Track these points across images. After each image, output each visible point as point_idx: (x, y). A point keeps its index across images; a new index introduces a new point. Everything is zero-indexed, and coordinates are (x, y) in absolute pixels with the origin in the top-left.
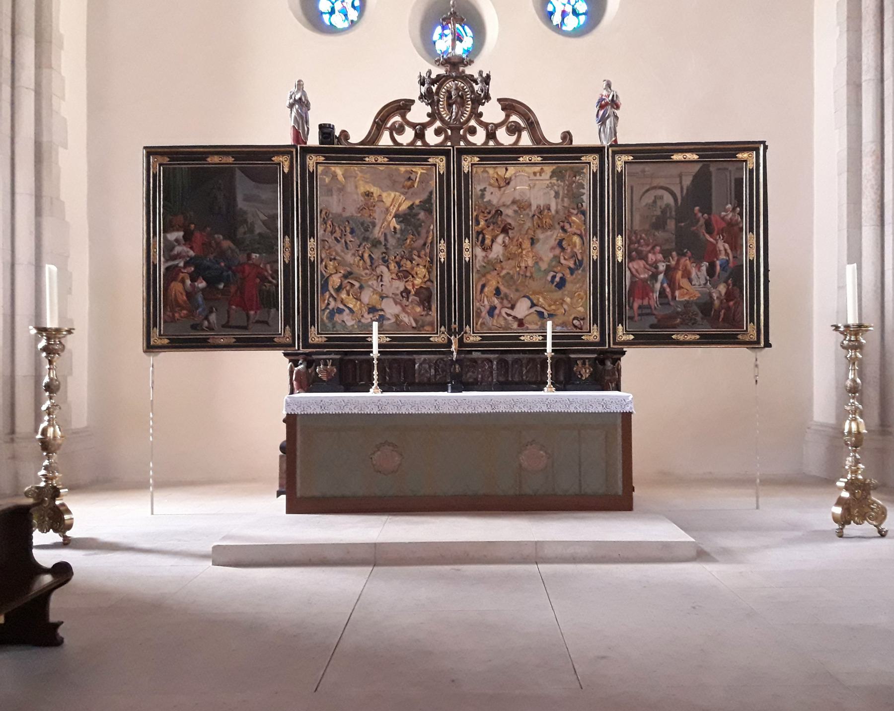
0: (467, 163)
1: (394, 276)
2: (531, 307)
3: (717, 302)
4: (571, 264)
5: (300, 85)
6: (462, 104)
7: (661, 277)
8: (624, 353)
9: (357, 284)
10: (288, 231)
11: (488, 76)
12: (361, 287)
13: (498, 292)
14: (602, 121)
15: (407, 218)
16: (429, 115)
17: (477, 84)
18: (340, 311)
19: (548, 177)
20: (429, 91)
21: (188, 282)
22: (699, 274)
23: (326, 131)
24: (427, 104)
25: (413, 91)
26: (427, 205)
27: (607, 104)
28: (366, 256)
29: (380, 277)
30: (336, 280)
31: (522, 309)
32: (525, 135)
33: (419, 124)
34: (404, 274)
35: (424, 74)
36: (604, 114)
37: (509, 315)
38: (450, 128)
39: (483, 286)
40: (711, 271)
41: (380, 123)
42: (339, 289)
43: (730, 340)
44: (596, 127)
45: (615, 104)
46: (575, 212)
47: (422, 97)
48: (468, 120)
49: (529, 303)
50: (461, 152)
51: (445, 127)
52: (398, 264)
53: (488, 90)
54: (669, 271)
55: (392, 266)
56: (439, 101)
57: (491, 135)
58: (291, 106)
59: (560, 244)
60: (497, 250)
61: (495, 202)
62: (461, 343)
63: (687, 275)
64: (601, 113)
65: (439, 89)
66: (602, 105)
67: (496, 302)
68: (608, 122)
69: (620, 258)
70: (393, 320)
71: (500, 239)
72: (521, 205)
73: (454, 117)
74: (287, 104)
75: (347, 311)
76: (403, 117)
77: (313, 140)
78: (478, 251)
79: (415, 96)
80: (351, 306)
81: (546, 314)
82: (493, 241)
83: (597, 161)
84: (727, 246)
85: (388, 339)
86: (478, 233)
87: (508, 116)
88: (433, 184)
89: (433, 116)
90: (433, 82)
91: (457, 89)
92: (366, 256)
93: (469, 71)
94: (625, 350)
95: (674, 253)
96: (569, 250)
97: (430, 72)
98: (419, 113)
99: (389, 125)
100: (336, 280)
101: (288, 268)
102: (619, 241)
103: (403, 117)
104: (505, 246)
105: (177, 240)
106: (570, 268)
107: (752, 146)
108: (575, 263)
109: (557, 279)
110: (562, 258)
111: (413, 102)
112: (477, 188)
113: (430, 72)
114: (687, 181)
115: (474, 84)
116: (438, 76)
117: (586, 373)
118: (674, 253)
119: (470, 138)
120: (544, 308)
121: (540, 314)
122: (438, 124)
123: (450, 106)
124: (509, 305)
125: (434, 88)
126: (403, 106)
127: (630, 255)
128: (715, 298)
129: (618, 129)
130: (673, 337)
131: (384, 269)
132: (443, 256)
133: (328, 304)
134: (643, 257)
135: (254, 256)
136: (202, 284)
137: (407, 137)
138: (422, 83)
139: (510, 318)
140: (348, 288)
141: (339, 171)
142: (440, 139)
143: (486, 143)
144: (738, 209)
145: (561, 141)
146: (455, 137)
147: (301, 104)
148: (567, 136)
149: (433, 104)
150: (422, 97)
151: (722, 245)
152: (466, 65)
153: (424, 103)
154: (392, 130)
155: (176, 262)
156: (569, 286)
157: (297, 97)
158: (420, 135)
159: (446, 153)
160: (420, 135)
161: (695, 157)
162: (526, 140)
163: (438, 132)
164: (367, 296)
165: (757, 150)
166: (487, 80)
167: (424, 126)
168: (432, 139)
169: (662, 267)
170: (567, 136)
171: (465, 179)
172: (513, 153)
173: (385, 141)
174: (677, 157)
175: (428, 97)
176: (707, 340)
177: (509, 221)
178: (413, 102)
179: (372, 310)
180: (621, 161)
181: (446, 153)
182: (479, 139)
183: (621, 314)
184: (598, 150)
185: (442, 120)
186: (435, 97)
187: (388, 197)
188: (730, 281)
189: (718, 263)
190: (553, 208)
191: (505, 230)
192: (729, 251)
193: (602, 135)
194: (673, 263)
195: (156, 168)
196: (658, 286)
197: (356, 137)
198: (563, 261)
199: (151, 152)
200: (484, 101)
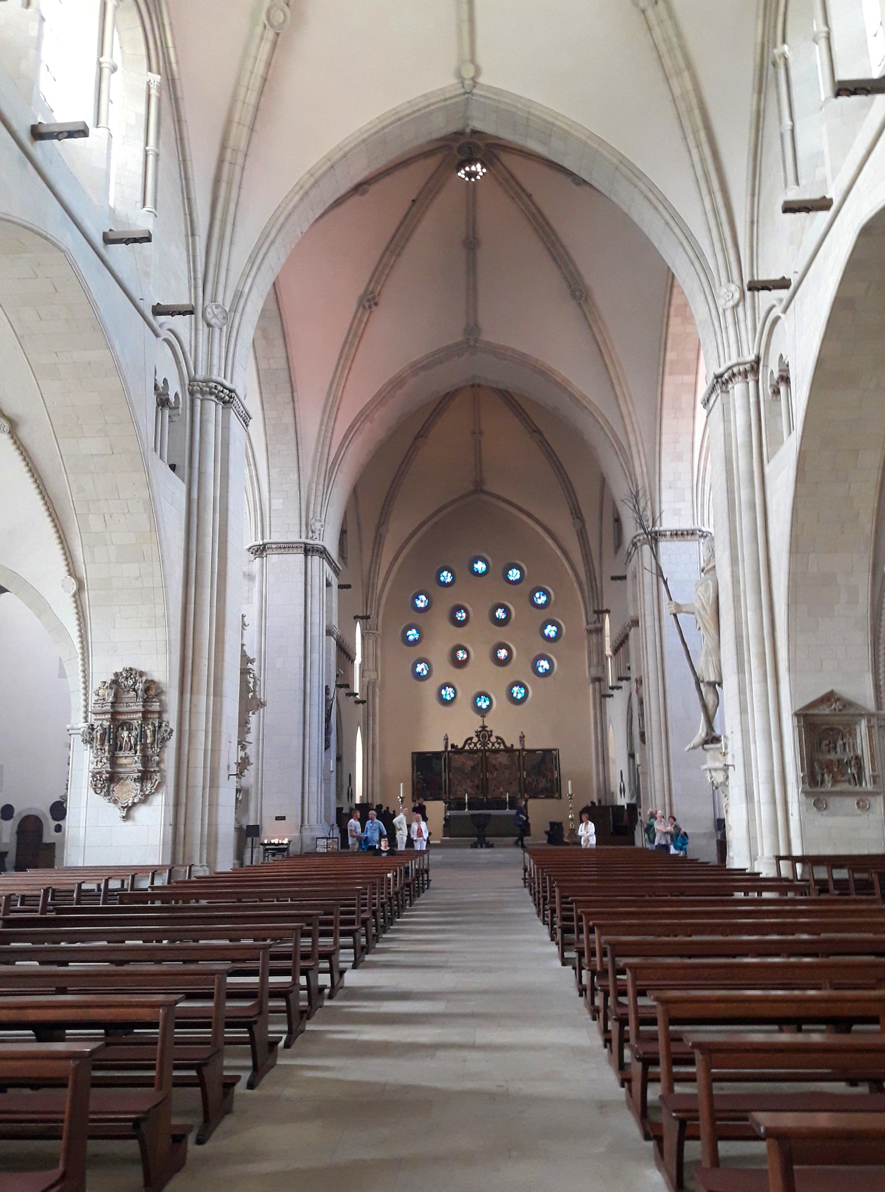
0: (487, 754)
5: (446, 735)
6: (486, 737)
10: (445, 771)
13: (495, 785)
14: (521, 741)
15: (473, 767)
22: (544, 780)
23: (453, 746)
25: (473, 735)
26: (478, 764)
30: (456, 783)
31: (502, 789)
34: (472, 781)
42: (457, 785)
43: (552, 797)
50: (486, 751)
57: (493, 745)
60: (495, 775)
62: (487, 798)
66: (520, 737)
72: (501, 764)
77: (449, 749)
88: (479, 759)
89: (479, 740)
93: (488, 729)
98: (475, 740)
100: (456, 783)
107: (555, 750)
112: (490, 760)
126: (471, 739)
127: (528, 775)
141: (456, 756)
146: (484, 746)
147: (446, 739)
148: (512, 745)
149: (479, 738)
151: (549, 774)
158: (475, 745)
160: (475, 745)
162: (502, 747)
164: (464, 787)
166: (491, 732)
168: (479, 746)
170: (512, 745)
171: (487, 758)
172: (497, 751)
173: (467, 748)
175: (478, 736)
176: (547, 797)
179: (465, 790)
180: (524, 753)
184: (518, 750)
187: (468, 762)
195: (414, 757)
197: (460, 746)
199: (413, 753)
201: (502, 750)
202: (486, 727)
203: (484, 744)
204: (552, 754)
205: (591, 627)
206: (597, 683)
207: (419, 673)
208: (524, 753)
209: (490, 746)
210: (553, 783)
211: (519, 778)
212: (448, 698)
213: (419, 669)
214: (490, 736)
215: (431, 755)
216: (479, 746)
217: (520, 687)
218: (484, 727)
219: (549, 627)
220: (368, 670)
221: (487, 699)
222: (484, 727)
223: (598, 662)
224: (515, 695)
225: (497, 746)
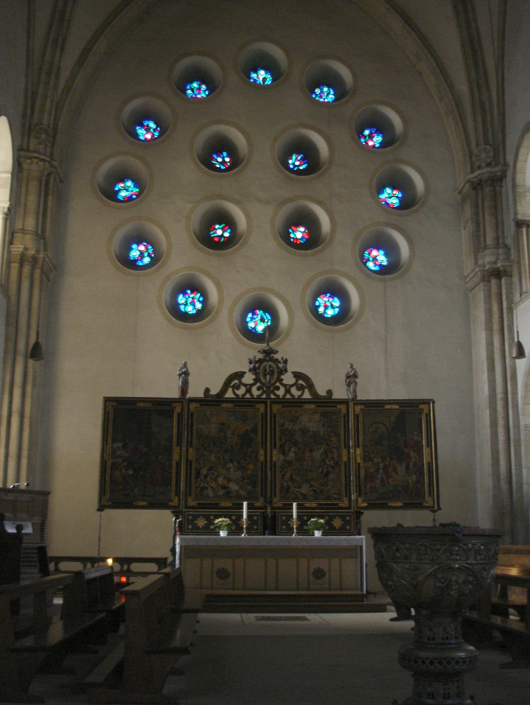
1: (236, 469)
2: (310, 487)
3: (411, 485)
4: (332, 463)
7: (381, 471)
8: (362, 513)
9: (216, 474)
10: (179, 443)
12: (218, 476)
13: (291, 478)
14: (349, 385)
16: (254, 380)
17: (280, 364)
18: (206, 488)
19: (318, 416)
21: (123, 470)
22: (401, 469)
24: (253, 374)
25: (245, 367)
26: (254, 430)
27: (351, 376)
28: (221, 458)
29: (228, 470)
30: (204, 472)
32: (306, 391)
33: (249, 385)
35: (252, 358)
36: (349, 382)
37: (298, 492)
38: (266, 387)
39: (284, 476)
40: (407, 468)
42: (206, 476)
44: (346, 387)
45: (355, 376)
46: (333, 435)
47: (250, 370)
48: (275, 382)
49: (309, 486)
50: (273, 402)
51: (262, 386)
52: (239, 462)
53: (286, 367)
54: (385, 468)
55: (236, 463)
56: (260, 372)
57: (288, 391)
58: (180, 375)
59: (326, 452)
60: (291, 455)
61: (290, 428)
63: (395, 470)
64: (348, 380)
65: (260, 366)
66: (348, 377)
67: (290, 484)
68: (352, 385)
69: (359, 461)
70: (236, 493)
71: (293, 449)
72: (304, 431)
73: (267, 381)
74: (178, 373)
75: (210, 488)
78: (282, 457)
79: (246, 369)
80: (212, 485)
81: (318, 491)
82: (289, 450)
83: (345, 408)
84: (415, 454)
85: (231, 504)
86: (282, 446)
89: (256, 380)
90: (256, 362)
91: (270, 366)
92: (221, 458)
93: (276, 356)
94: (362, 511)
95: (388, 458)
96: (330, 456)
97: (255, 357)
98: (249, 378)
99: (232, 385)
101: (178, 464)
102: (358, 451)
104: (295, 453)
105: (118, 448)
106: (331, 466)
107: (427, 402)
108: (334, 464)
109: (325, 472)
110: (327, 460)
111: (245, 373)
113: (255, 357)
114: (393, 419)
115: (279, 364)
116: (259, 359)
118: (388, 458)
119: (277, 392)
120: (317, 488)
121: (315, 491)
122: (259, 384)
123: (265, 376)
124: (297, 486)
125: (257, 365)
126: (239, 375)
128: (410, 483)
129: (357, 389)
130: (389, 504)
131: (230, 465)
132: (262, 458)
133: (200, 484)
134: (371, 460)
135: (160, 457)
136: (131, 472)
137: (241, 391)
138: (251, 362)
139: (298, 494)
140: (211, 475)
143: (285, 395)
144: (420, 435)
145: (326, 394)
147: (185, 374)
148: (330, 392)
149: (256, 374)
150: (250, 370)
151: (412, 454)
152: (275, 353)
153: (251, 374)
155: (118, 460)
156: (331, 476)
157: (184, 370)
158: (249, 391)
159: (265, 403)
160: (249, 391)
161: (397, 407)
162: (307, 395)
163: (259, 389)
164: (220, 480)
165: (429, 404)
166: (286, 361)
167: (252, 385)
168: (255, 392)
169: (381, 466)
170: (330, 392)
171: (274, 417)
172: (299, 402)
173: (229, 394)
174: (387, 407)
175: (253, 370)
177: (299, 439)
178: (245, 373)
180: (358, 408)
181: (265, 403)
182: (281, 392)
183: (360, 491)
184: (345, 402)
185: (261, 383)
186: (258, 371)
188: (418, 474)
189: (411, 463)
190: (322, 432)
191: (295, 444)
192: (416, 457)
193: (349, 393)
194: (388, 463)
196: (379, 476)
198: (327, 462)
199: (107, 400)
200: (284, 372)
201: (307, 402)
204: (421, 412)
205: (484, 172)
206: (494, 282)
207: (135, 261)
208: (358, 408)
209: (281, 392)
210: (422, 474)
211: (347, 464)
212: (190, 310)
213: (134, 254)
215: (149, 405)
216: (255, 392)
217: (333, 296)
219: (388, 190)
220: (23, 231)
221: (268, 317)
223: (497, 238)
224: (321, 310)
225: (294, 390)
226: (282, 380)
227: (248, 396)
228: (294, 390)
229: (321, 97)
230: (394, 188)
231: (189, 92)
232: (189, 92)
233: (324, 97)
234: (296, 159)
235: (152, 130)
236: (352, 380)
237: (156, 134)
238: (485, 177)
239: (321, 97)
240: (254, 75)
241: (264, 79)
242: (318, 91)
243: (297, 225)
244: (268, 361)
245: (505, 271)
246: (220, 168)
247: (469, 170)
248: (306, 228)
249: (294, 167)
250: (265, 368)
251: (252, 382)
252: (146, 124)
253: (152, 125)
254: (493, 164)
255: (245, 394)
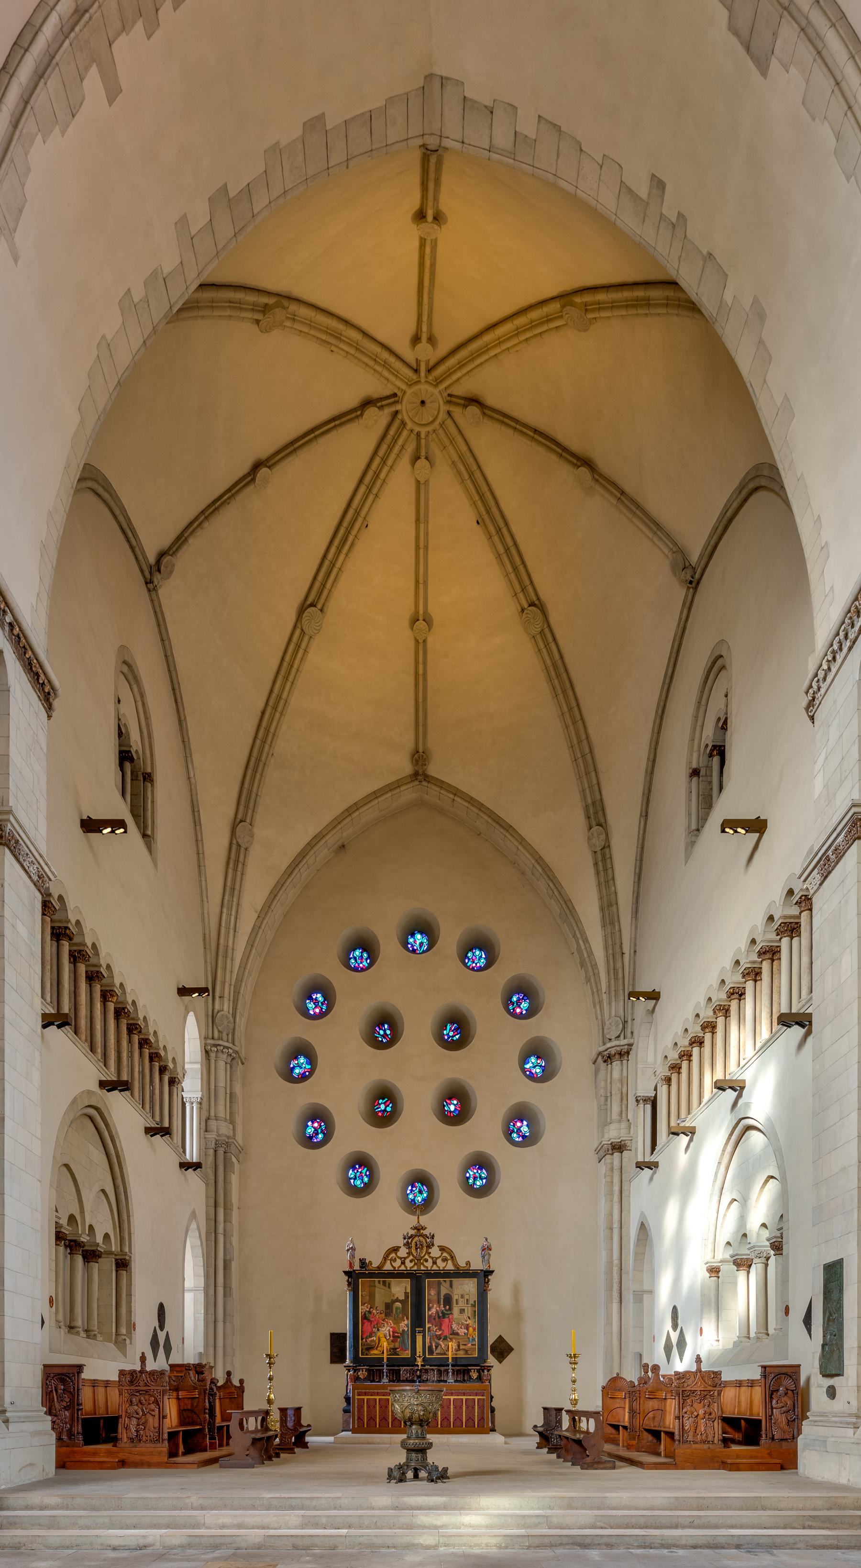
6: (422, 1249)
11: (433, 1235)
14: (483, 1257)
20: (408, 1242)
23: (363, 1263)
25: (400, 1242)
32: (450, 1262)
41: (385, 1258)
44: (481, 1259)
47: (404, 1245)
48: (425, 1255)
57: (434, 1263)
58: (348, 1250)
76: (396, 1254)
77: (357, 1267)
87: (442, 1254)
89: (409, 1253)
90: (409, 1238)
98: (403, 1252)
103: (396, 1254)
117: (474, 1375)
119: (425, 1263)
122: (411, 1257)
123: (416, 1249)
125: (410, 1241)
126: (396, 1249)
138: (405, 1239)
142: (413, 1263)
143: (432, 1267)
148: (468, 1263)
149: (410, 1248)
154: (391, 1260)
158: (403, 1263)
160: (403, 1263)
162: (450, 1266)
163: (411, 1261)
166: (433, 1237)
167: (405, 1258)
168: (409, 1265)
170: (468, 1263)
173: (388, 1267)
175: (407, 1245)
182: (429, 1264)
185: (413, 1256)
202: (424, 1228)
203: (418, 1260)
206: (617, 1155)
214: (430, 1246)
218: (419, 1229)
222: (419, 1229)
226: (430, 1253)
227: (403, 1268)
228: (439, 1262)
229: (473, 962)
230: (538, 1058)
231: (353, 961)
232: (353, 961)
233: (476, 962)
234: (451, 1029)
235: (320, 1004)
236: (487, 1251)
237: (324, 1007)
238: (613, 1051)
239: (473, 962)
240: (411, 940)
241: (421, 944)
242: (470, 955)
243: (450, 1099)
244: (419, 1236)
245: (625, 1145)
246: (382, 1041)
247: (601, 1043)
248: (458, 1101)
249: (449, 1038)
250: (416, 1243)
251: (406, 1255)
252: (314, 997)
253: (319, 997)
254: (622, 1036)
255: (400, 1267)
